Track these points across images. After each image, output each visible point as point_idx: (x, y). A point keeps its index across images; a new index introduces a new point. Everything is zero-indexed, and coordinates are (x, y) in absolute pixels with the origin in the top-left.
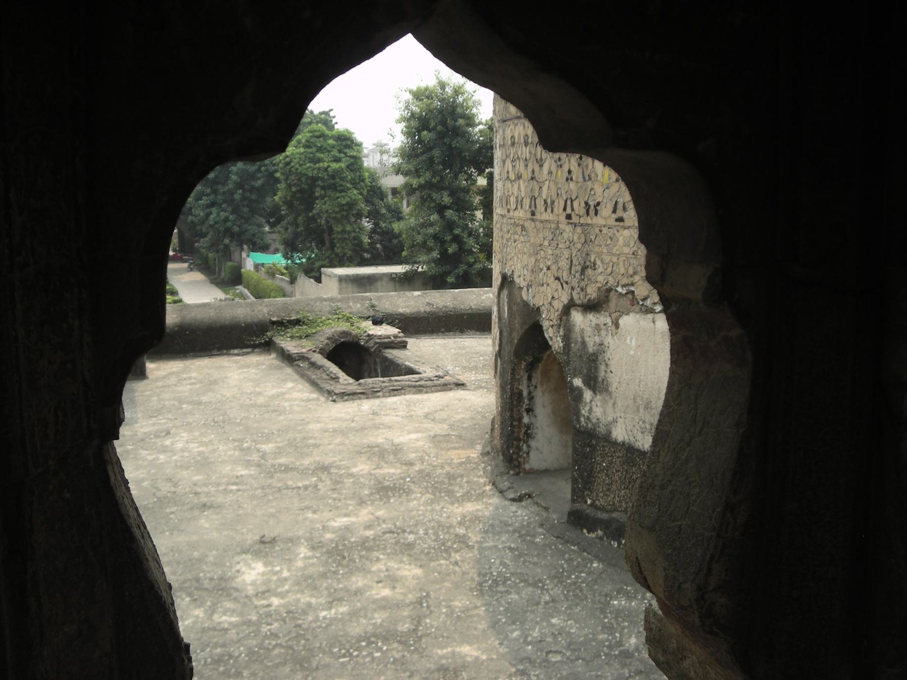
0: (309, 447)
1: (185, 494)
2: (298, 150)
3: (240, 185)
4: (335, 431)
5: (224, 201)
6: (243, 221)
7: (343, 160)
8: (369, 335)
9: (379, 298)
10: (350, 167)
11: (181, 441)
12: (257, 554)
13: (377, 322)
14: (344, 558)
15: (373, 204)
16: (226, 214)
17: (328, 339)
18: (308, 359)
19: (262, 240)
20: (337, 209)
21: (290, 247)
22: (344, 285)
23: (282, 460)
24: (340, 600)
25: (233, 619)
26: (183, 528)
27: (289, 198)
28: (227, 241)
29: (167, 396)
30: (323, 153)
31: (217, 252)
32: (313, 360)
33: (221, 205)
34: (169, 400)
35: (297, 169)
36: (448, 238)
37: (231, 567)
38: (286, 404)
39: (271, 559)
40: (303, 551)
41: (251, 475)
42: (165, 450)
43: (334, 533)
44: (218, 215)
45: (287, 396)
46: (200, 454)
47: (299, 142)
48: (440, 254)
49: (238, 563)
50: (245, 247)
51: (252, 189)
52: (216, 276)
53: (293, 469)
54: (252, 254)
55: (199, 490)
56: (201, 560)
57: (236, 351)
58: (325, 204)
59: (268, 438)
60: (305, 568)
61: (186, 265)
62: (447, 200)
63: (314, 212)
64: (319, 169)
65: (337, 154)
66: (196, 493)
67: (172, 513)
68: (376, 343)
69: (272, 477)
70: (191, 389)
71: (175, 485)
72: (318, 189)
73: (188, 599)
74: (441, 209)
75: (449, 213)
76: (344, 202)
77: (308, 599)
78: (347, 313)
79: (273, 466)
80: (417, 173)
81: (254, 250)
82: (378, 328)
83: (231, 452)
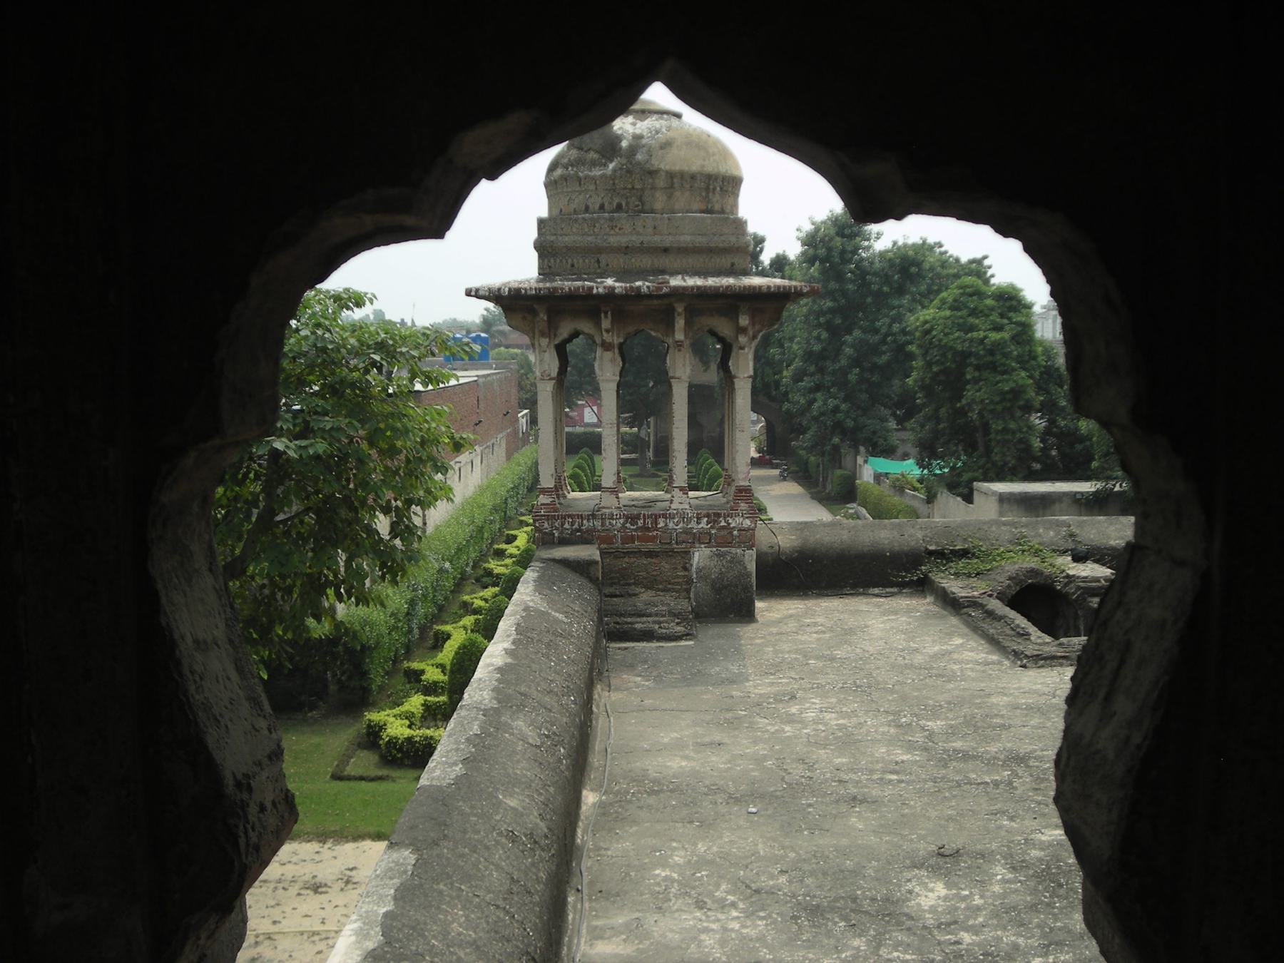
0: (994, 728)
1: (826, 780)
3: (856, 362)
4: (1029, 708)
5: (833, 385)
6: (859, 412)
7: (1007, 328)
8: (1068, 576)
9: (1081, 525)
11: (811, 708)
12: (936, 871)
13: (1079, 558)
14: (1061, 886)
16: (836, 402)
17: (1010, 579)
18: (982, 606)
20: (997, 399)
21: (927, 452)
22: (1006, 506)
23: (958, 744)
24: (1060, 944)
25: (908, 957)
26: (827, 827)
27: (927, 381)
28: (836, 440)
29: (786, 647)
31: (823, 454)
32: (989, 607)
33: (829, 388)
34: (789, 652)
35: (940, 340)
37: (900, 886)
38: (956, 667)
39: (956, 879)
40: (1000, 871)
41: (917, 761)
42: (791, 719)
43: (1042, 849)
45: (955, 656)
46: (841, 727)
47: (943, 301)
49: (909, 880)
50: (862, 449)
51: (875, 367)
52: (819, 488)
53: (974, 758)
54: (871, 458)
55: (846, 777)
56: (856, 872)
57: (876, 591)
58: (979, 390)
59: (935, 713)
60: (1004, 896)
61: (776, 472)
63: (964, 401)
64: (972, 340)
66: (840, 781)
67: (810, 805)
68: (1079, 588)
69: (945, 766)
70: (818, 639)
71: (811, 768)
73: (843, 924)
77: (1013, 938)
78: (1034, 542)
79: (945, 751)
81: (875, 453)
82: (1081, 566)
83: (886, 729)
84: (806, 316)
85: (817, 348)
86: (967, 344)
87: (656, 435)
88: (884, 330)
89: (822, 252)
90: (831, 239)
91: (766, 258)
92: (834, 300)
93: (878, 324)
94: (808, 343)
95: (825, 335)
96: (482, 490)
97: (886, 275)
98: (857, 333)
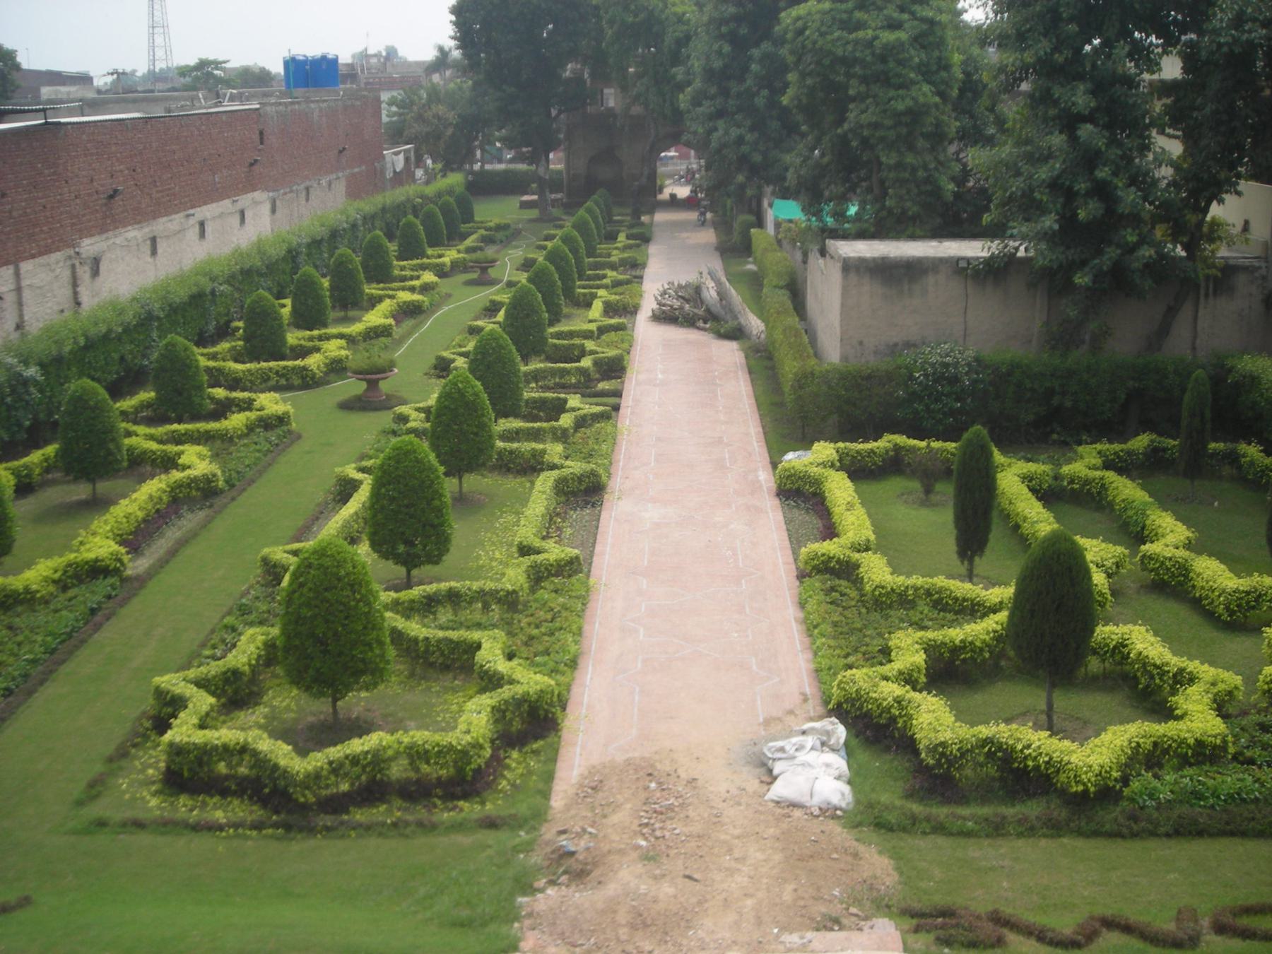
2: (820, 6)
7: (906, 25)
10: (919, 40)
16: (739, 132)
20: (888, 122)
21: (811, 193)
22: (853, 277)
27: (804, 101)
28: (740, 178)
35: (815, 43)
36: (1082, 186)
44: (726, 133)
54: (778, 203)
58: (863, 112)
61: (693, 216)
62: (1081, 98)
63: (846, 126)
64: (857, 42)
65: (895, 15)
74: (1070, 122)
75: (1086, 131)
76: (901, 106)
85: (717, 64)
86: (850, 48)
94: (708, 58)
95: (727, 48)
96: (259, 247)
98: (766, 46)
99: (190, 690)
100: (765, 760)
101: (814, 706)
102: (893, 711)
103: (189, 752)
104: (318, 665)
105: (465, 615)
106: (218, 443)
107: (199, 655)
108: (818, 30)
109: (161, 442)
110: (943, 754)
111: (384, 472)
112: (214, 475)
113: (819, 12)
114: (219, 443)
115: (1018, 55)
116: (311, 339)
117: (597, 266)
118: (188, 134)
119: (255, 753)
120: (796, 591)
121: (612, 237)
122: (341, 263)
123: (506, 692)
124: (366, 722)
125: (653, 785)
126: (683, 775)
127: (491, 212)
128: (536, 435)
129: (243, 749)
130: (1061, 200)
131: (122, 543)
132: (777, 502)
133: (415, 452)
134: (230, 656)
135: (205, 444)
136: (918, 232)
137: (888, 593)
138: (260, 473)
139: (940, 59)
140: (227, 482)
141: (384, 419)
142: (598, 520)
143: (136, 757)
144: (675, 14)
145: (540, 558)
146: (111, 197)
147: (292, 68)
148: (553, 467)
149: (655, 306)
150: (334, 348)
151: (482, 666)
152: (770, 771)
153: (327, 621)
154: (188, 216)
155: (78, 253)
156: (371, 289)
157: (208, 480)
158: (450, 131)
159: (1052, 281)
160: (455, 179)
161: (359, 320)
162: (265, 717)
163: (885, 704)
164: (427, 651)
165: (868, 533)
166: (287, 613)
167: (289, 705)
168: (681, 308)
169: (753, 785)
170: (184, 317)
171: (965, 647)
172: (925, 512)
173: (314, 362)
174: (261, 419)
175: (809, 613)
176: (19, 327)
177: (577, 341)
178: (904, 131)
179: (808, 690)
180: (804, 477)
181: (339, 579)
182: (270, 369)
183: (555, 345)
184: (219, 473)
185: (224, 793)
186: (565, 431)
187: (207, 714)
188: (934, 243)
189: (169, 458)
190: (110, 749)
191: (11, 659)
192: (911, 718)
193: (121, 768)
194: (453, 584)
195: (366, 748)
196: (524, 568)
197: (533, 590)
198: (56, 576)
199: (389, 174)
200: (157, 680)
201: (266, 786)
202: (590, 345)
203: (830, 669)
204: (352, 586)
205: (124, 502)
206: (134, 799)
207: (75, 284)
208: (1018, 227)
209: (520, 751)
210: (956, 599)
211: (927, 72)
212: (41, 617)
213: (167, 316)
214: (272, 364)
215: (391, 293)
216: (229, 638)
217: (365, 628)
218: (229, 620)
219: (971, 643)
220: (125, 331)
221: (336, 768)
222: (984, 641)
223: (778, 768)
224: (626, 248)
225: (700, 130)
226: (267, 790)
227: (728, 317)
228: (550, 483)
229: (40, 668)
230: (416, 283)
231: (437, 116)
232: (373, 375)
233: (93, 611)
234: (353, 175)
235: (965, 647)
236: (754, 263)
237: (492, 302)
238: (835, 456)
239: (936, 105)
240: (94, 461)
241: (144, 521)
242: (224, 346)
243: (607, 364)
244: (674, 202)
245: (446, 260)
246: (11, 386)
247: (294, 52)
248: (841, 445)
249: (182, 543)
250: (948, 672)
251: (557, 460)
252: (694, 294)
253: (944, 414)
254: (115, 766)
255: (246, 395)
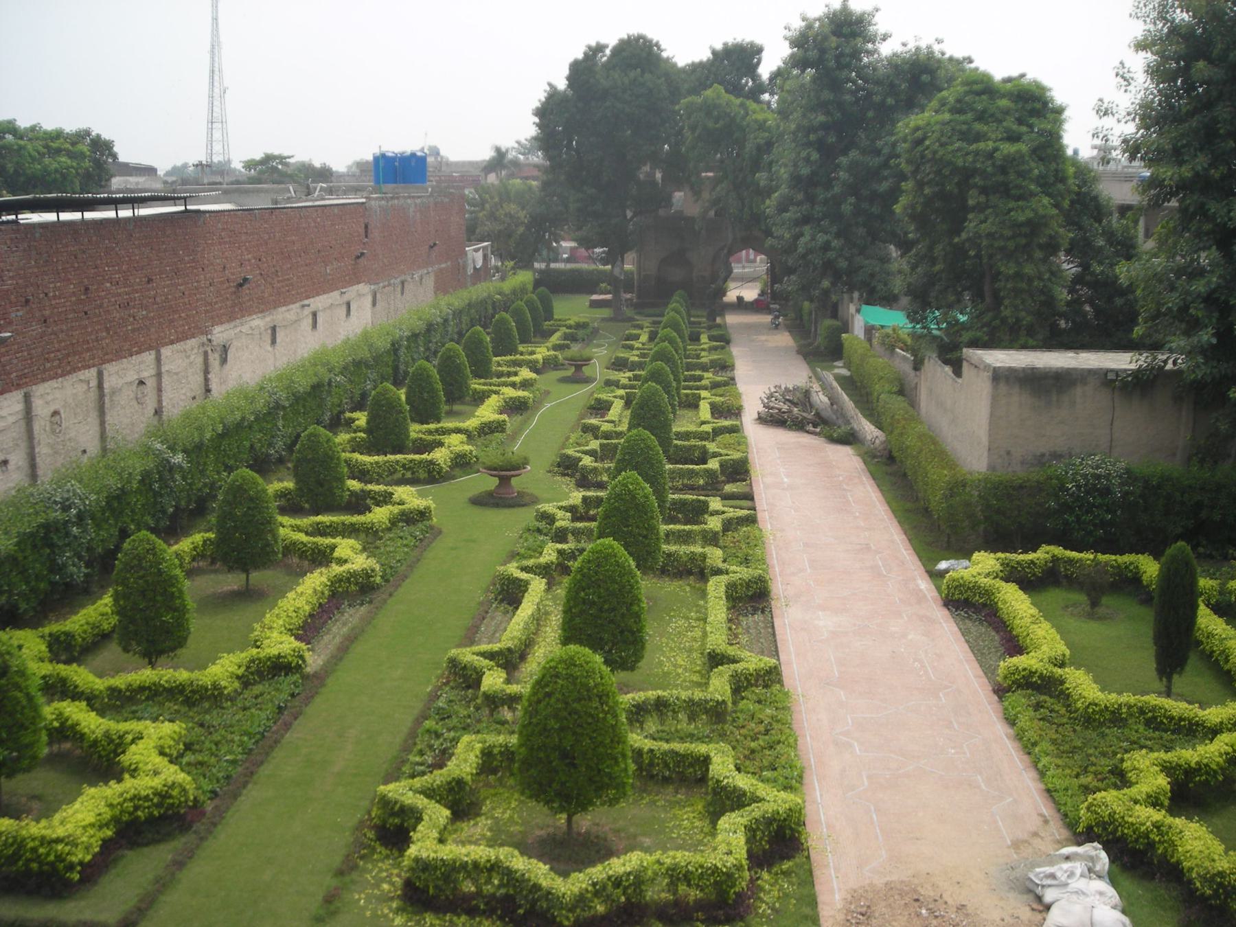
2: (940, 117)
7: (1025, 138)
15: (1080, 228)
16: (826, 238)
19: (886, 284)
21: (919, 301)
22: (1003, 388)
27: (919, 208)
30: (986, 124)
33: (820, 220)
35: (935, 153)
44: (813, 239)
47: (943, 103)
48: (1217, 335)
50: (856, 295)
54: (865, 308)
58: (982, 222)
61: (767, 319)
63: (964, 235)
64: (977, 153)
65: (1015, 127)
72: (973, 192)
80: (1177, 155)
84: (794, 133)
85: (805, 171)
86: (970, 158)
87: (639, 274)
88: (886, 151)
89: (813, 54)
90: (825, 38)
91: (765, 70)
92: (828, 113)
93: (879, 144)
94: (795, 165)
95: (815, 156)
97: (892, 85)
98: (854, 154)
99: (421, 801)
100: (1031, 886)
101: (1057, 829)
102: (1152, 836)
103: (436, 868)
104: (563, 779)
105: (670, 725)
106: (363, 536)
107: (404, 762)
108: (939, 140)
109: (307, 534)
110: (1220, 885)
111: (583, 575)
112: (373, 571)
113: (937, 123)
114: (370, 537)
115: (1176, 169)
116: (430, 432)
117: (690, 367)
118: (278, 229)
119: (509, 873)
120: (998, 707)
121: (695, 338)
122: (449, 358)
123: (756, 811)
124: (597, 837)
125: (924, 911)
126: (950, 902)
127: (571, 310)
128: (685, 538)
129: (494, 867)
130: (1216, 315)
131: (298, 638)
132: (946, 612)
133: (615, 556)
134: (451, 764)
135: (349, 537)
136: (1031, 342)
137: (1101, 711)
138: (411, 567)
139: (1056, 171)
140: (382, 577)
141: (526, 516)
142: (773, 627)
143: (366, 871)
144: (756, 121)
145: (739, 667)
146: (241, 285)
147: (381, 164)
148: (718, 572)
149: (761, 408)
150: (456, 443)
151: (718, 781)
152: (1039, 899)
153: (575, 733)
154: (303, 306)
155: (210, 341)
156: (476, 385)
157: (367, 574)
158: (521, 229)
159: (1201, 395)
160: (524, 277)
161: (472, 415)
162: (490, 829)
163: (1143, 828)
164: (651, 764)
165: (1061, 648)
166: (530, 723)
167: (511, 817)
168: (790, 412)
169: (1025, 914)
170: (304, 406)
171: (1200, 769)
172: (1093, 626)
173: (440, 456)
174: (403, 513)
175: (1023, 730)
176: (158, 412)
177: (693, 442)
178: (1023, 241)
179: (1045, 812)
180: (975, 588)
181: (588, 691)
182: (397, 462)
183: (676, 446)
184: (377, 567)
185: (472, 912)
186: (716, 533)
187: (445, 828)
188: (1071, 354)
189: (320, 551)
190: (337, 860)
191: (213, 760)
192: (1173, 844)
193: (353, 882)
194: (660, 692)
195: (629, 869)
196: (726, 677)
197: (734, 703)
198: (240, 672)
199: (470, 271)
200: (382, 788)
201: (520, 906)
202: (712, 447)
203: (1066, 789)
204: (600, 697)
205: (291, 595)
206: (375, 916)
207: (206, 372)
208: (1179, 342)
209: (769, 872)
210: (1171, 718)
211: (1045, 184)
212: (230, 714)
213: (291, 405)
214: (399, 457)
215: (494, 388)
216: (436, 744)
217: (612, 741)
218: (428, 724)
219: (1207, 765)
220: (257, 419)
221: (599, 890)
222: (1218, 764)
223: (1049, 896)
224: (712, 349)
225: (787, 236)
226: (521, 911)
227: (840, 421)
228: (723, 589)
229: (240, 769)
230: (517, 379)
231: (511, 216)
232: (506, 471)
233: (280, 709)
234: (441, 270)
235: (1200, 769)
236: (848, 366)
237: (598, 401)
238: (998, 567)
239: (1052, 217)
240: (246, 550)
241: (311, 615)
242: (343, 437)
243: (732, 466)
244: (741, 305)
245: (539, 357)
246: (159, 472)
247: (384, 149)
248: (1000, 555)
249: (350, 640)
250: (1189, 793)
251: (721, 565)
252: (803, 398)
253: (1095, 525)
254: (347, 879)
255: (382, 488)
